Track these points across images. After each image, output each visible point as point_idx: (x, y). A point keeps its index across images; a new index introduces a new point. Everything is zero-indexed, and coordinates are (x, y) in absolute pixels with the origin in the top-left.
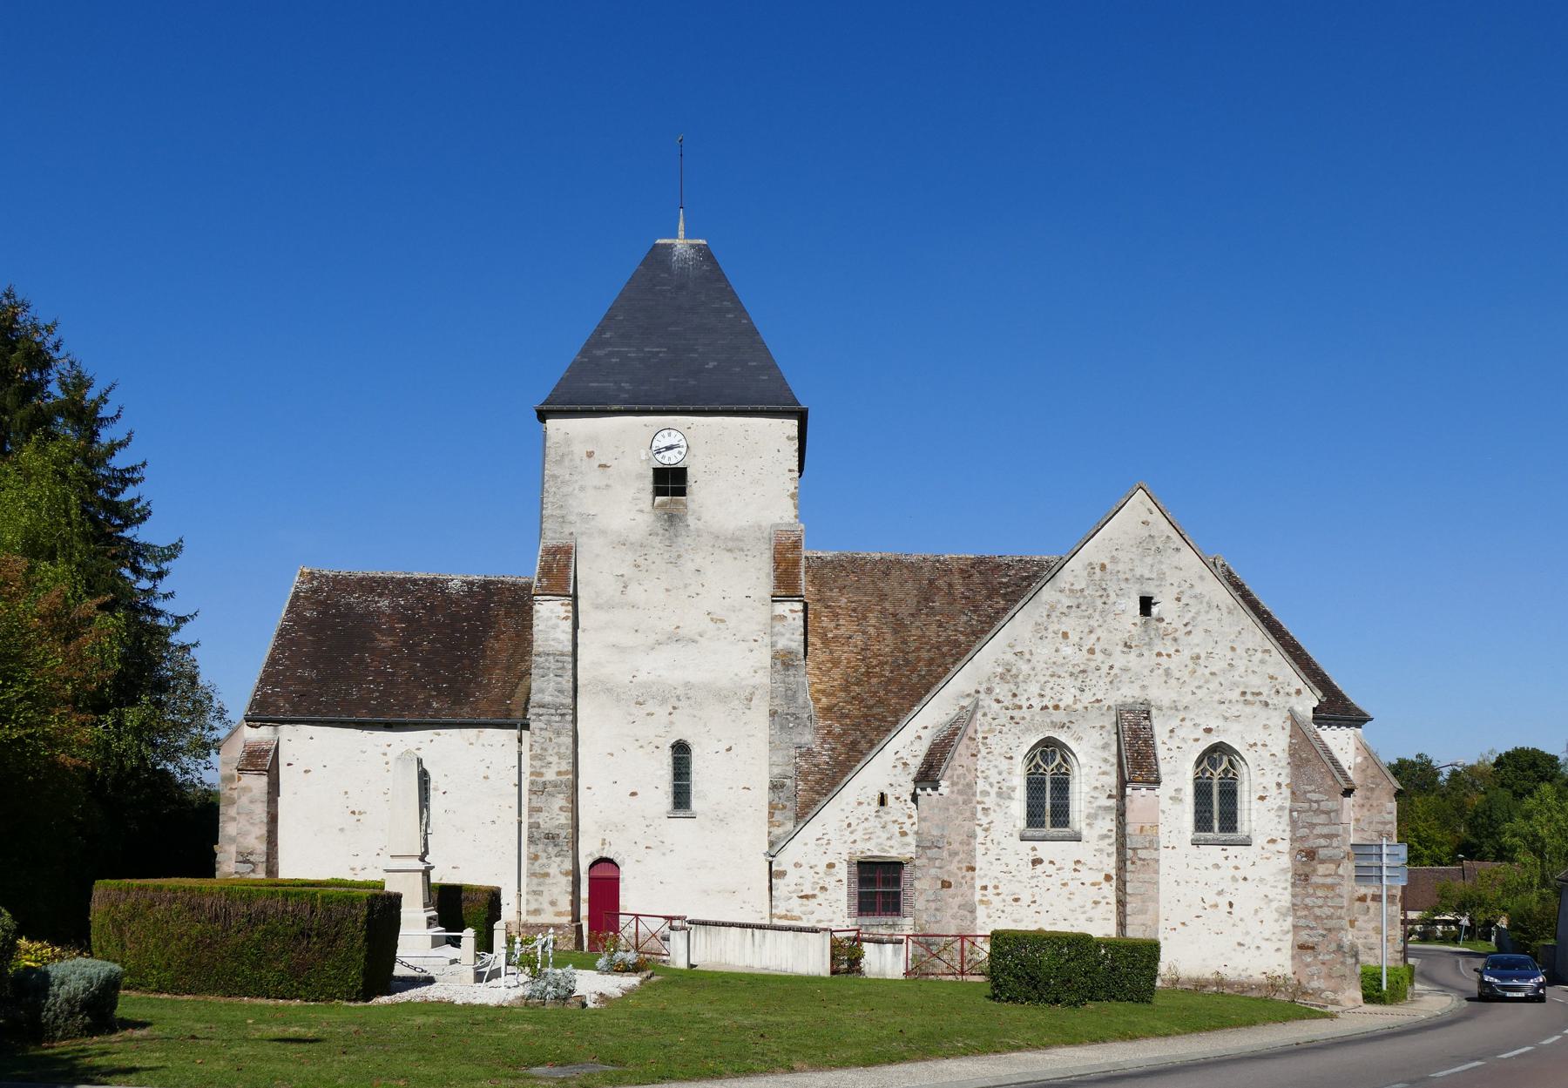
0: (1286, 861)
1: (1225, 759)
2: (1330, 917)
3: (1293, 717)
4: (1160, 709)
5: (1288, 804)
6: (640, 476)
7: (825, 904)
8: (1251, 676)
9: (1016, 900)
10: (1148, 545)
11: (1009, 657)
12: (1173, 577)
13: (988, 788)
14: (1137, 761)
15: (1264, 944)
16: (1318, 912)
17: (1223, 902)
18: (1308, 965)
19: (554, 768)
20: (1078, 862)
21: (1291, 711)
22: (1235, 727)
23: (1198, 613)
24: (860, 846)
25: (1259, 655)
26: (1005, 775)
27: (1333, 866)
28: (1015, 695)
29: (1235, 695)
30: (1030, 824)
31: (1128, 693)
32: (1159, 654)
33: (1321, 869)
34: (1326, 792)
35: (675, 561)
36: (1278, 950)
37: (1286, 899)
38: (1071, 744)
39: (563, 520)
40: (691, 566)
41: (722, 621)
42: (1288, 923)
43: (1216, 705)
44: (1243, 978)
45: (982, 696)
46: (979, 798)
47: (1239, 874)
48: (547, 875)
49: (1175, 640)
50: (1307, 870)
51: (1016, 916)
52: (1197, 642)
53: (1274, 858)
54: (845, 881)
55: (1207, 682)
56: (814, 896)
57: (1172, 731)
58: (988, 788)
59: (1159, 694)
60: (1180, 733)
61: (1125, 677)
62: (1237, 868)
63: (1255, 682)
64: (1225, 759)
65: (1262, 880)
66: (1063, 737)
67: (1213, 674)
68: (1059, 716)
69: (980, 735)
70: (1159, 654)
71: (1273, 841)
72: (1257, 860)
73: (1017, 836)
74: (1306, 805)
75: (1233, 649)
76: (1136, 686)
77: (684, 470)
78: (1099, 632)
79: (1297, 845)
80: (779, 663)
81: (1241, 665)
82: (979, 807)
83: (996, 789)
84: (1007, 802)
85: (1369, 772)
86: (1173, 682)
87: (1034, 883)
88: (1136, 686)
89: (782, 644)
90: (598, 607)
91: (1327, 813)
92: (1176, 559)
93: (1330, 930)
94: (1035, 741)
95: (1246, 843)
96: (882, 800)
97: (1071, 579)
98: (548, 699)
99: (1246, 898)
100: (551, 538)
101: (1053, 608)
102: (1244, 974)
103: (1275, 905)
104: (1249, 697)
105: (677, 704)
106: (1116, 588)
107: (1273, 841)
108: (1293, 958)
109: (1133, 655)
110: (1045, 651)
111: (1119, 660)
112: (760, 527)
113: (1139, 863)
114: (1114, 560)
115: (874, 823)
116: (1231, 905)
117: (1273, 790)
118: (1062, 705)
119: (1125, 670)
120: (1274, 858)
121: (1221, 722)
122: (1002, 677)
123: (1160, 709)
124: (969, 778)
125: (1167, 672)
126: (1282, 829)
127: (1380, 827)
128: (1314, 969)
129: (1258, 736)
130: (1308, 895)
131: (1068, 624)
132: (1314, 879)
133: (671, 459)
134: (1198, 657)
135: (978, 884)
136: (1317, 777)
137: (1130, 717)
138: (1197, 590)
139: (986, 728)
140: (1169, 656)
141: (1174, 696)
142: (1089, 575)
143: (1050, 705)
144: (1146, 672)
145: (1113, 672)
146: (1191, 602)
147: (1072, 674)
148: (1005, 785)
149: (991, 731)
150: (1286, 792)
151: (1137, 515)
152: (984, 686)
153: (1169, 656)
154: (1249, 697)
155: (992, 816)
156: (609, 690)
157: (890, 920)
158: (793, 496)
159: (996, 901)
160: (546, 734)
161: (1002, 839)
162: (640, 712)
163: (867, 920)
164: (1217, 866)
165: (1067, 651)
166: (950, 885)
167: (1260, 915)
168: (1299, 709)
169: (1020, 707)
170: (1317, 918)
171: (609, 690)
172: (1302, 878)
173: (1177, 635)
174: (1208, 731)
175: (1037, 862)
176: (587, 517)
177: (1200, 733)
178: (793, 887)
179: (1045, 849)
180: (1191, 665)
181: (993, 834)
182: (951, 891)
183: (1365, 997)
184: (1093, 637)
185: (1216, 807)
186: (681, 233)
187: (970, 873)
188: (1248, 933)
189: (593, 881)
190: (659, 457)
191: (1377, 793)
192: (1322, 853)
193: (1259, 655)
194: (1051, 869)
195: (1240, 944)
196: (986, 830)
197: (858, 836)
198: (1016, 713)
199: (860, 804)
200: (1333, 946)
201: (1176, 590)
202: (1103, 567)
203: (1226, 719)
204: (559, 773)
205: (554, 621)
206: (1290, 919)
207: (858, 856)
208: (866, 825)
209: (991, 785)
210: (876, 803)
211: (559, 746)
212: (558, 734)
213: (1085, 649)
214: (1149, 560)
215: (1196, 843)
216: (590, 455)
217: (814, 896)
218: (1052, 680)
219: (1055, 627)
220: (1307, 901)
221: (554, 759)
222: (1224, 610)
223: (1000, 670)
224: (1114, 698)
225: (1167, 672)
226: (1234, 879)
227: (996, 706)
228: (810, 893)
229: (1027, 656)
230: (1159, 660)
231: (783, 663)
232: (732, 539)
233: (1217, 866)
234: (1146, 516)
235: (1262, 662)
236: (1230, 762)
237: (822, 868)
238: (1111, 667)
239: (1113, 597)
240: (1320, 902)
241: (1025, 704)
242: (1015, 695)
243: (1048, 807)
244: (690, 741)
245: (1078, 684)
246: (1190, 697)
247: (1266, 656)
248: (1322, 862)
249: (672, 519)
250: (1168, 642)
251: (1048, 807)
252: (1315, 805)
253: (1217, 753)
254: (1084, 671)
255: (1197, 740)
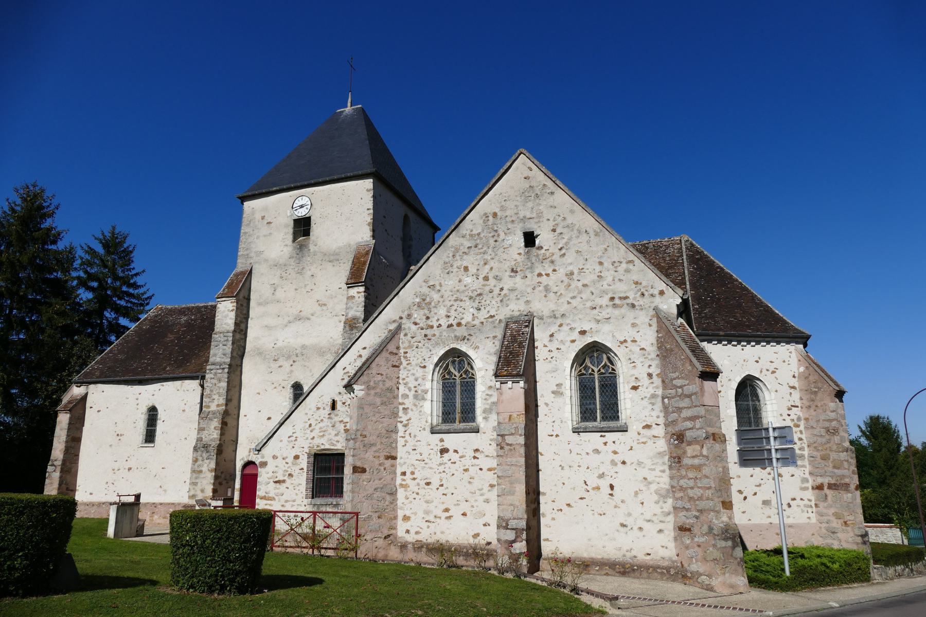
0: (662, 445)
1: (605, 356)
2: (700, 498)
3: (658, 314)
4: (541, 318)
5: (660, 392)
6: (286, 226)
7: (291, 487)
8: (618, 284)
9: (428, 484)
10: (530, 193)
11: (425, 290)
12: (548, 214)
13: (407, 392)
14: (517, 358)
15: (646, 526)
16: (691, 493)
17: (604, 484)
18: (687, 548)
19: (216, 403)
20: (477, 450)
21: (656, 309)
22: (606, 328)
23: (570, 239)
24: (317, 441)
25: (624, 265)
26: (420, 381)
27: (698, 447)
28: (428, 318)
29: (605, 301)
30: (445, 421)
31: (515, 308)
32: (540, 275)
33: (690, 450)
34: (686, 377)
35: (300, 273)
36: (660, 531)
37: (664, 481)
38: (471, 353)
39: (247, 256)
40: (309, 273)
41: (325, 305)
42: (669, 504)
43: (588, 311)
44: (628, 559)
45: (404, 321)
46: (400, 400)
47: (618, 458)
48: (201, 472)
49: (552, 262)
50: (680, 452)
51: (428, 498)
52: (571, 261)
53: (650, 443)
54: (305, 470)
55: (580, 292)
56: (284, 481)
57: (552, 335)
58: (407, 392)
59: (540, 306)
60: (559, 336)
61: (512, 296)
62: (615, 453)
63: (622, 288)
64: (605, 356)
65: (640, 463)
66: (464, 348)
67: (585, 285)
68: (461, 332)
69: (402, 351)
70: (540, 275)
71: (648, 427)
72: (635, 445)
73: (428, 429)
74: (673, 391)
75: (601, 263)
76: (522, 302)
77: (309, 218)
78: (492, 263)
79: (670, 429)
80: (347, 326)
81: (609, 276)
82: (401, 407)
83: (413, 392)
84: (421, 403)
85: (811, 378)
86: (551, 295)
87: (441, 468)
88: (522, 302)
89: (351, 314)
90: (260, 304)
91: (689, 396)
92: (551, 200)
93: (701, 511)
94: (442, 352)
95: (624, 430)
96: (334, 406)
97: (471, 227)
98: (218, 360)
99: (626, 481)
100: (241, 265)
101: (457, 250)
102: (628, 554)
103: (654, 487)
104: (617, 301)
105: (295, 359)
106: (504, 228)
107: (648, 427)
108: (676, 539)
109: (518, 279)
110: (451, 282)
111: (508, 283)
112: (350, 245)
113: (507, 448)
114: (503, 208)
115: (327, 423)
116: (612, 487)
117: (645, 381)
118: (463, 322)
119: (512, 290)
120: (650, 443)
121: (593, 325)
122: (419, 305)
123: (541, 318)
124: (389, 384)
125: (547, 289)
126: (655, 415)
127: (827, 424)
128: (690, 552)
129: (627, 333)
130: (682, 477)
131: (468, 261)
132: (686, 461)
133: (302, 213)
134: (572, 273)
135: (399, 470)
136: (679, 364)
137: (514, 326)
138: (569, 221)
139: (406, 345)
140: (548, 275)
141: (552, 306)
142: (484, 222)
143: (454, 323)
144: (529, 290)
145: (503, 293)
146: (565, 231)
147: (471, 298)
148: (420, 389)
149: (410, 347)
150: (657, 381)
151: (523, 171)
152: (406, 313)
153: (548, 275)
154: (617, 301)
155: (410, 414)
156: (260, 354)
157: (334, 501)
158: (369, 224)
159: (412, 484)
160: (214, 381)
161: (418, 433)
162: (274, 365)
163: (318, 501)
164: (597, 451)
165: (468, 280)
166: (364, 471)
167: (640, 497)
168: (664, 307)
169: (432, 327)
170: (691, 499)
171: (260, 354)
172: (676, 460)
173: (554, 258)
174: (583, 333)
175: (444, 451)
176: (259, 253)
177: (575, 335)
178: (271, 474)
179: (451, 440)
180: (566, 280)
181: (412, 429)
182: (364, 476)
183: (752, 581)
184: (487, 267)
185: (598, 401)
186: (349, 104)
187: (390, 462)
188: (629, 515)
189: (243, 476)
190: (296, 213)
191: (820, 395)
192: (689, 434)
193: (624, 265)
194: (455, 457)
195: (623, 525)
196: (405, 426)
197: (316, 433)
198: (429, 332)
199: (318, 408)
200: (705, 529)
201: (552, 223)
202: (495, 215)
203: (598, 321)
204: (218, 406)
205: (226, 312)
206: (670, 501)
207: (315, 449)
208: (321, 425)
209: (410, 389)
210: (328, 408)
211: (219, 388)
212: (220, 381)
213: (481, 277)
214: (530, 205)
215: (576, 431)
216: (263, 218)
217: (284, 481)
218: (456, 304)
219: (459, 263)
220: (682, 482)
221: (216, 397)
222: (592, 234)
223: (418, 300)
224: (504, 313)
225: (547, 289)
226: (613, 463)
227: (414, 327)
228: (281, 478)
229: (438, 288)
230: (540, 279)
231: (350, 326)
232: (333, 255)
233: (597, 451)
234: (527, 173)
235: (627, 271)
236: (609, 358)
237: (290, 459)
238: (502, 289)
239: (502, 236)
240: (691, 483)
241: (435, 324)
242: (428, 318)
243: (458, 405)
244: (302, 383)
245: (476, 305)
246: (566, 306)
247: (631, 266)
248: (690, 444)
249: (301, 248)
250: (547, 264)
251: (458, 405)
252: (680, 390)
253: (593, 354)
254: (480, 295)
255: (573, 341)
